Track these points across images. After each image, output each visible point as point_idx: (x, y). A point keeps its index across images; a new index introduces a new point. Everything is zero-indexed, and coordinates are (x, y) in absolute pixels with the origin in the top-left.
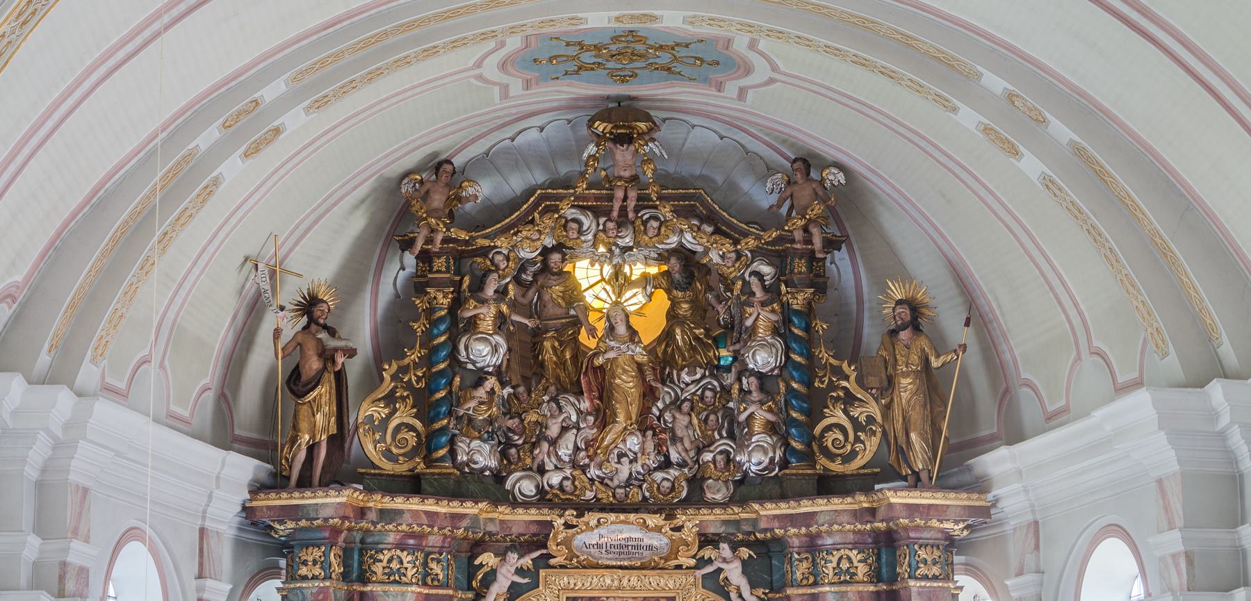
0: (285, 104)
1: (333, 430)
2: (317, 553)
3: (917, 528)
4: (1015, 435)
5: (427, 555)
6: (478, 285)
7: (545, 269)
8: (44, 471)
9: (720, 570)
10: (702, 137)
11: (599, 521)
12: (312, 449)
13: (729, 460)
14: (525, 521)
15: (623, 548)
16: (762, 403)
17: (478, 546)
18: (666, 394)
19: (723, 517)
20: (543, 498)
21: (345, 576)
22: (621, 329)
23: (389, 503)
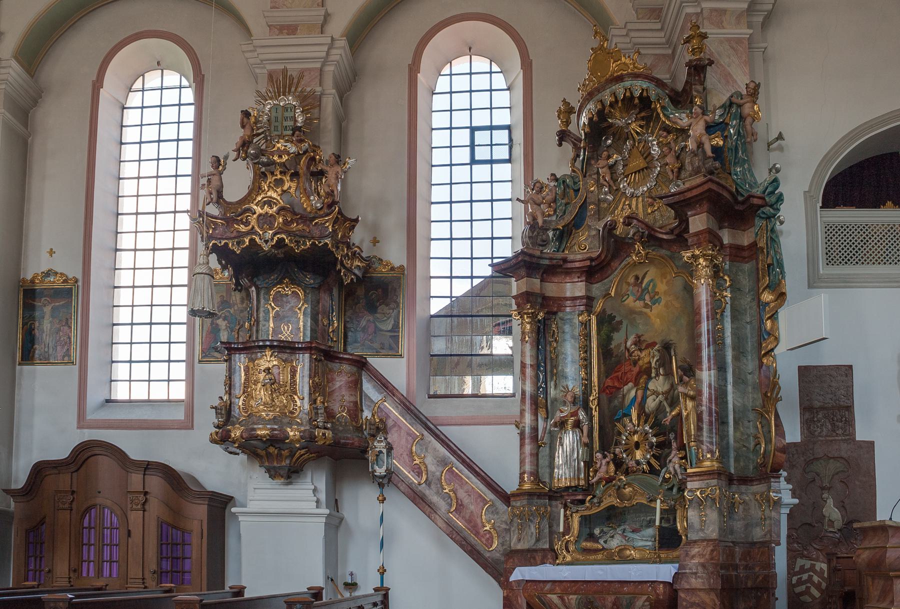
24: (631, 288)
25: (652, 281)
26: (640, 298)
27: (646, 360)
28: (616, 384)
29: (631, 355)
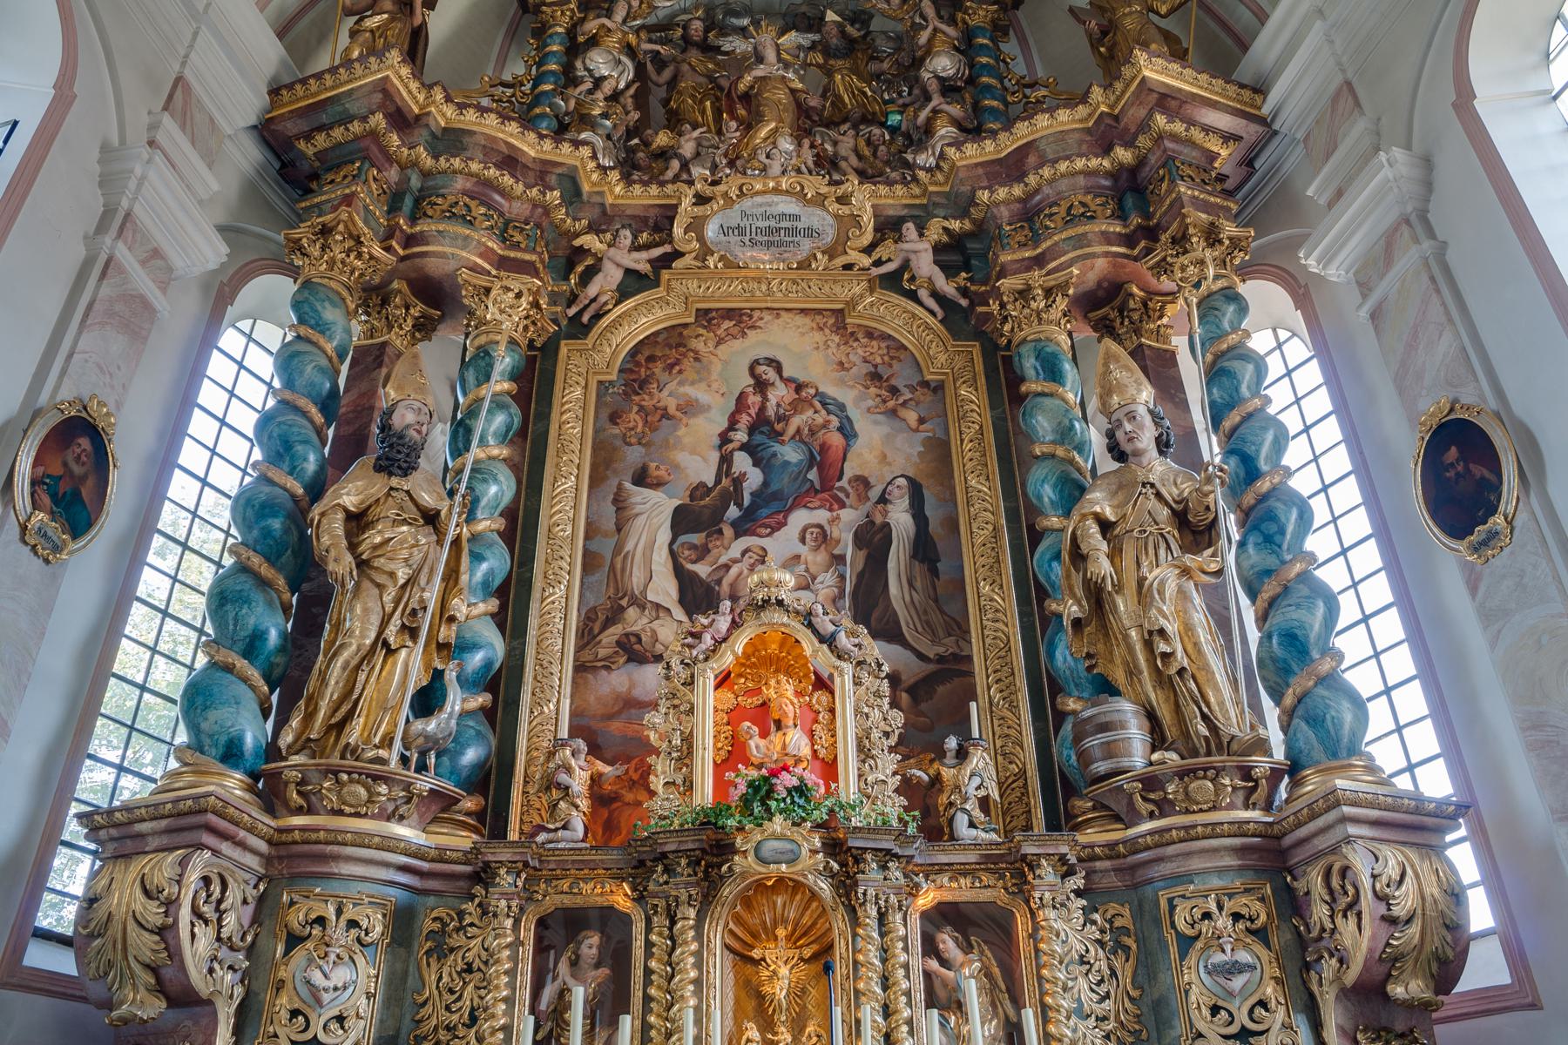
5: (507, 223)
9: (905, 265)
11: (740, 189)
14: (644, 206)
19: (904, 202)
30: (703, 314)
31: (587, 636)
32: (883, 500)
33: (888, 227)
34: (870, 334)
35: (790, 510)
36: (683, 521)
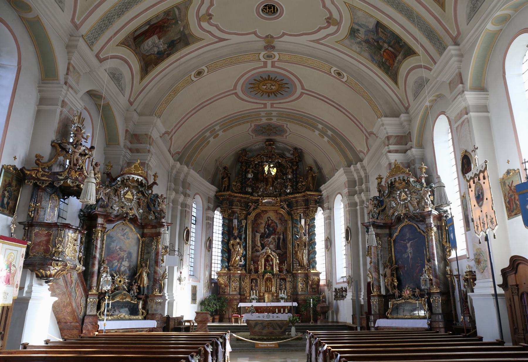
0: (219, 130)
1: (228, 184)
2: (226, 202)
3: (311, 198)
4: (324, 182)
6: (249, 166)
7: (259, 165)
8: (184, 180)
10: (281, 145)
12: (225, 187)
13: (285, 191)
15: (269, 203)
16: (289, 182)
17: (249, 203)
18: (276, 182)
20: (258, 196)
21: (229, 205)
22: (269, 173)
23: (236, 195)
24: (120, 231)
25: (127, 232)
26: (123, 236)
27: (123, 255)
28: (111, 259)
29: (117, 252)
30: (262, 211)
31: (252, 249)
32: (280, 235)
33: (281, 201)
34: (280, 213)
35: (271, 236)
36: (261, 237)
